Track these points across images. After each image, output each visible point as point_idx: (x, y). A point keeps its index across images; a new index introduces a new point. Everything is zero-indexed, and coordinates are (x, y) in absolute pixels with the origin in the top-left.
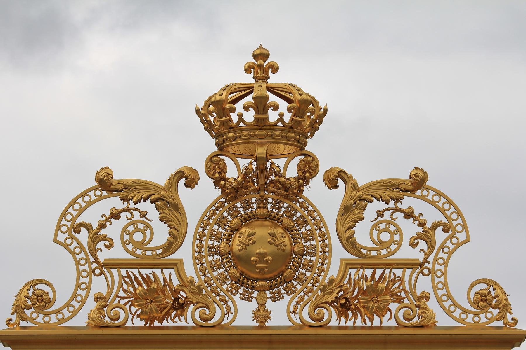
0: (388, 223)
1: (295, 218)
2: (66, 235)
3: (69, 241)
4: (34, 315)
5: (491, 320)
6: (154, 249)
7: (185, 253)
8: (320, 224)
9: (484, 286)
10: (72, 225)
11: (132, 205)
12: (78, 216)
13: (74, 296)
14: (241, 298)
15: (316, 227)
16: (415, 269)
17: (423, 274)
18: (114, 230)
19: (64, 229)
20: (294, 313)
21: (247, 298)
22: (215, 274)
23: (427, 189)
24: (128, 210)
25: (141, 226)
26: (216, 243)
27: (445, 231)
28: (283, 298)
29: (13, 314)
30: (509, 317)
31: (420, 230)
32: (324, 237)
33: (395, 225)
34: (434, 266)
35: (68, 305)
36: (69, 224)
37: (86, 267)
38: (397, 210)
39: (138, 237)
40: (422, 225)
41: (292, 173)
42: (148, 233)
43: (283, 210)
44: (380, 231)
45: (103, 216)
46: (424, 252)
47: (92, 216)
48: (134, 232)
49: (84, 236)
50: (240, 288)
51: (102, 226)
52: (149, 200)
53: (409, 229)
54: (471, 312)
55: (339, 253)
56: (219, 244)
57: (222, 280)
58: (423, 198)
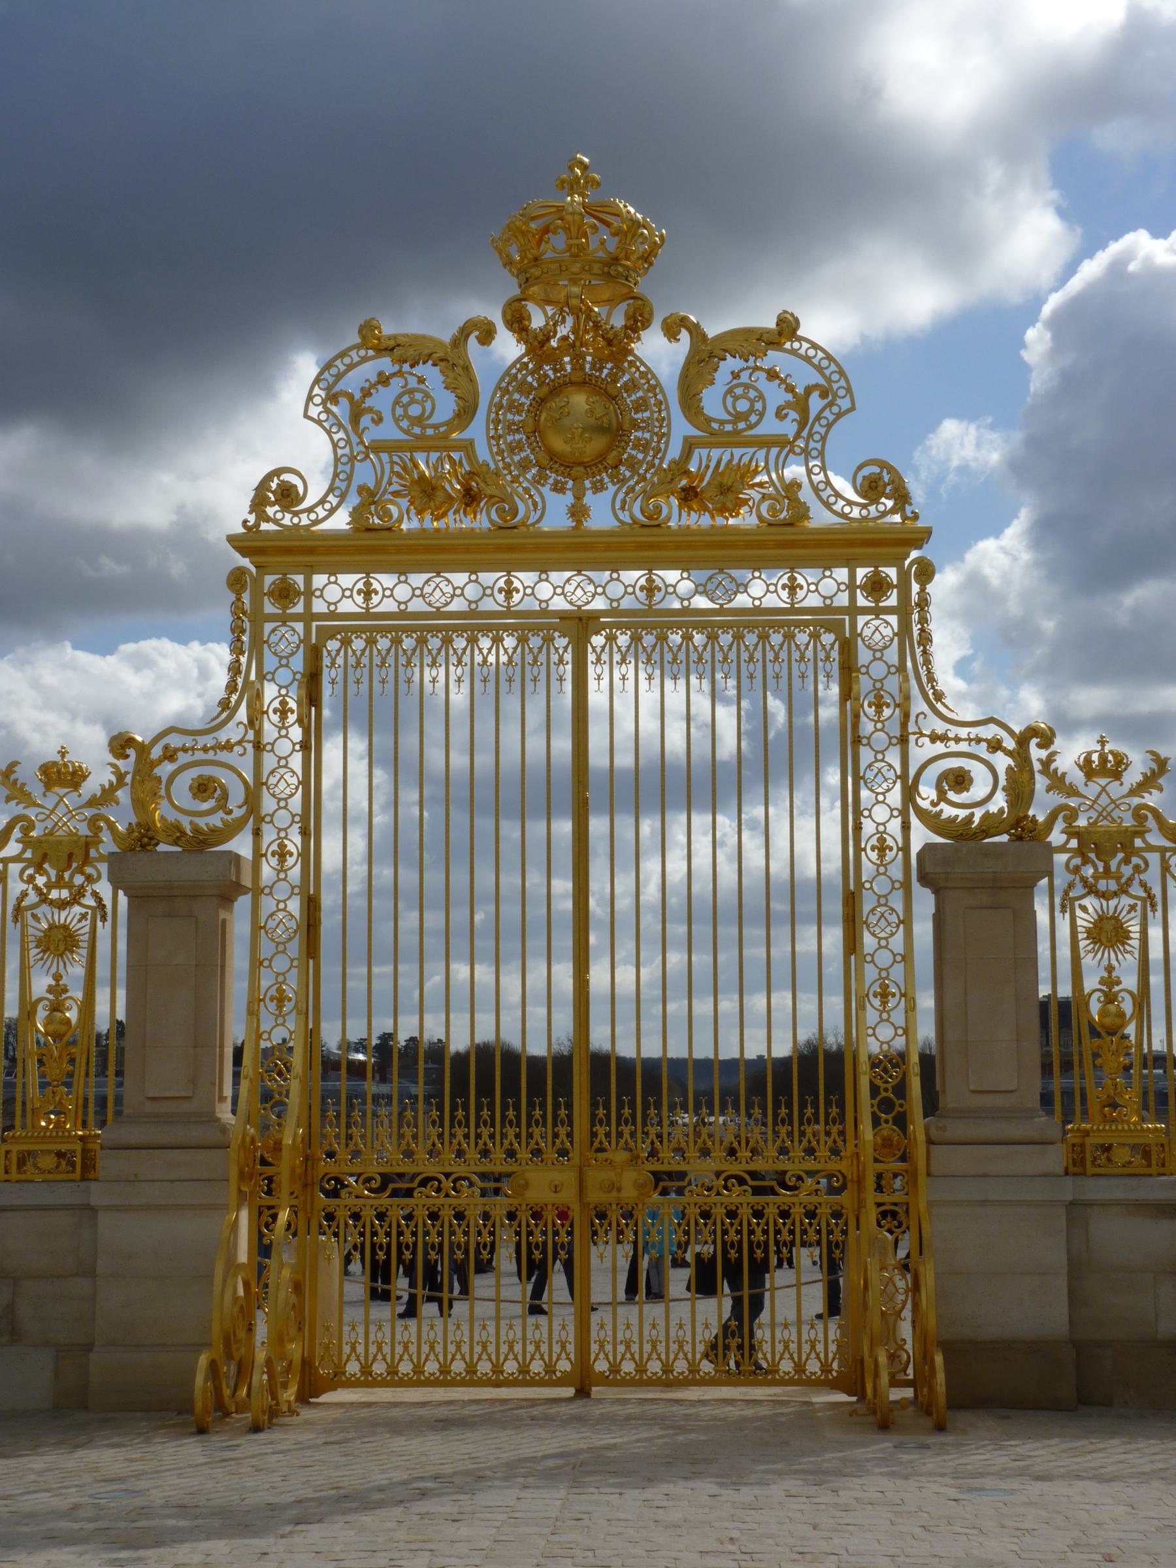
0: (747, 386)
2: (320, 408)
5: (884, 514)
6: (436, 427)
7: (477, 430)
8: (655, 388)
11: (406, 367)
12: (336, 383)
16: (782, 448)
17: (794, 453)
19: (317, 400)
21: (558, 488)
22: (517, 458)
23: (801, 339)
24: (400, 373)
25: (418, 396)
27: (824, 395)
29: (250, 513)
30: (908, 509)
31: (789, 397)
33: (756, 390)
34: (807, 445)
35: (322, 502)
39: (415, 410)
40: (790, 389)
41: (618, 321)
42: (428, 405)
43: (605, 371)
45: (367, 380)
51: (366, 393)
52: (430, 362)
53: (776, 396)
57: (524, 466)
58: (794, 352)
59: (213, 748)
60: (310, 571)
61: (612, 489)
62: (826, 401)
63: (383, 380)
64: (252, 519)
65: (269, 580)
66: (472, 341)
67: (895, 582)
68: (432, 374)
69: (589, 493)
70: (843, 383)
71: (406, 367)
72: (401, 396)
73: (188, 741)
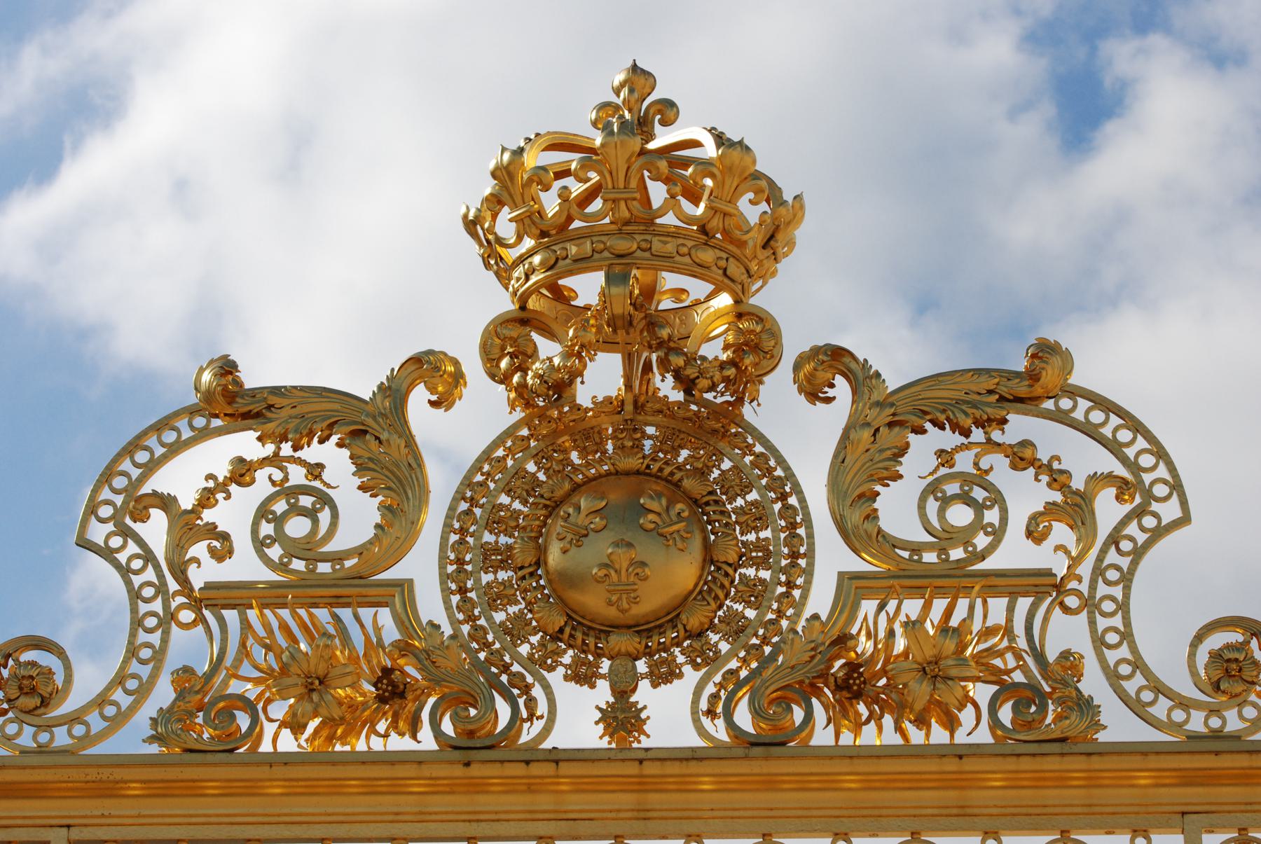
0: (965, 479)
1: (716, 473)
2: (110, 527)
3: (116, 542)
6: (337, 558)
8: (784, 484)
9: (1235, 637)
11: (286, 450)
12: (142, 479)
14: (566, 678)
15: (773, 495)
16: (1039, 596)
18: (235, 514)
19: (106, 511)
20: (711, 713)
21: (583, 676)
24: (274, 460)
25: (306, 501)
26: (503, 540)
28: (680, 676)
31: (1057, 497)
32: (795, 521)
33: (988, 487)
34: (1093, 587)
35: (101, 701)
36: (119, 500)
37: (157, 606)
38: (992, 445)
39: (297, 527)
42: (325, 517)
43: (684, 453)
44: (946, 502)
46: (1067, 552)
48: (285, 515)
49: (156, 529)
50: (565, 652)
51: (206, 499)
53: (1026, 495)
54: (1198, 705)
55: (832, 559)
56: (511, 541)
57: (515, 631)
58: (1062, 417)
61: (691, 676)
62: (1128, 508)
63: (242, 472)
66: (419, 398)
68: (332, 456)
69: (644, 685)
70: (1162, 472)
71: (286, 450)
72: (271, 499)
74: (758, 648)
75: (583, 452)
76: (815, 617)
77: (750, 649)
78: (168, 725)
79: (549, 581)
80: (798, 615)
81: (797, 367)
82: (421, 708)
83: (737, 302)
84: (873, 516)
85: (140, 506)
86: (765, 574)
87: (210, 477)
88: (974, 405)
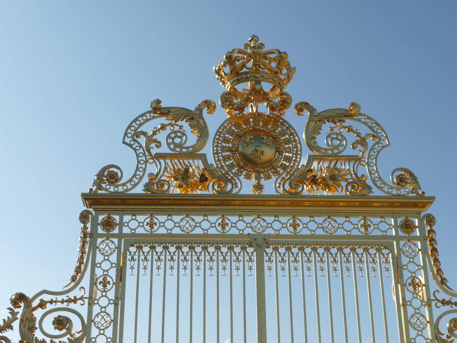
0: (337, 134)
2: (131, 139)
3: (132, 143)
4: (108, 187)
5: (408, 193)
6: (187, 148)
10: (134, 133)
11: (173, 122)
13: (135, 175)
18: (162, 137)
19: (129, 135)
21: (248, 177)
23: (360, 115)
24: (170, 124)
28: (271, 178)
29: (93, 186)
33: (342, 136)
35: (130, 181)
36: (133, 132)
37: (144, 158)
39: (177, 140)
40: (358, 135)
42: (184, 138)
44: (333, 139)
47: (148, 128)
48: (174, 137)
49: (142, 140)
51: (154, 133)
54: (395, 188)
58: (359, 120)
59: (67, 301)
60: (122, 213)
61: (274, 178)
63: (163, 127)
64: (94, 188)
65: (101, 218)
66: (205, 111)
67: (417, 225)
68: (185, 124)
73: (54, 297)
74: (289, 172)
75: (246, 125)
76: (303, 165)
77: (288, 172)
78: (147, 187)
79: (239, 155)
80: (299, 164)
81: (296, 107)
82: (209, 185)
83: (281, 91)
84: (315, 142)
85: (137, 134)
86: (291, 155)
87: (155, 128)
88: (338, 117)
